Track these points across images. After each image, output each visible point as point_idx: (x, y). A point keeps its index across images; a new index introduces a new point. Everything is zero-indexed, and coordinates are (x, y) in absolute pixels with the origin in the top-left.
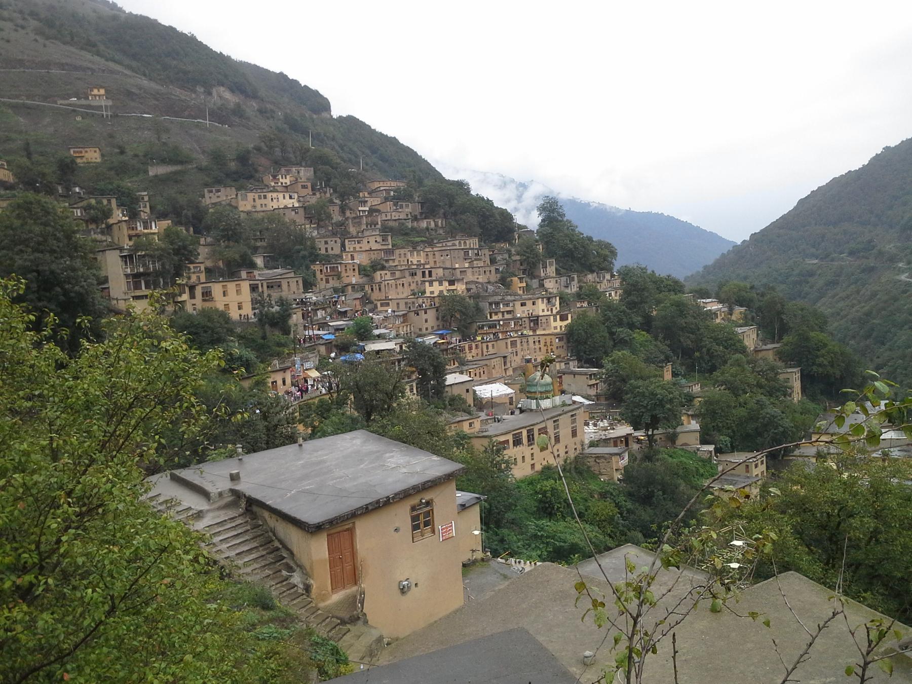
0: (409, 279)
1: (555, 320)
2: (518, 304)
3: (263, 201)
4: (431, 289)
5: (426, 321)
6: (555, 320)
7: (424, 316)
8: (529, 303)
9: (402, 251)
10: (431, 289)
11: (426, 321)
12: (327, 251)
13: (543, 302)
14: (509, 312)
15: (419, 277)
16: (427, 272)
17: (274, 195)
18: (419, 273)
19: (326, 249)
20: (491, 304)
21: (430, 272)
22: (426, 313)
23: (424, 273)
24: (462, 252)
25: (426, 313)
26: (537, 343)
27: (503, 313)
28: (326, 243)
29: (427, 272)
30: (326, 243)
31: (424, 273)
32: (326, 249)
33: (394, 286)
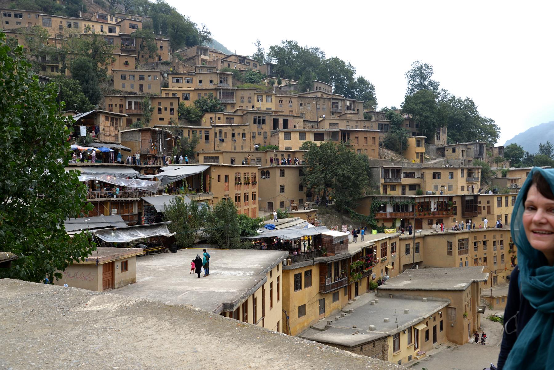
0: (255, 128)
1: (499, 205)
2: (428, 175)
4: (287, 143)
5: (282, 189)
6: (499, 205)
7: (280, 181)
8: (445, 175)
9: (246, 94)
10: (287, 143)
11: (282, 189)
13: (462, 176)
14: (412, 187)
15: (268, 127)
16: (281, 122)
18: (269, 122)
19: (141, 86)
20: (386, 171)
21: (285, 122)
22: (282, 174)
23: (276, 122)
24: (330, 104)
25: (282, 174)
26: (498, 246)
27: (404, 187)
28: (142, 78)
29: (281, 122)
30: (142, 78)
31: (276, 122)
32: (141, 86)
33: (229, 136)
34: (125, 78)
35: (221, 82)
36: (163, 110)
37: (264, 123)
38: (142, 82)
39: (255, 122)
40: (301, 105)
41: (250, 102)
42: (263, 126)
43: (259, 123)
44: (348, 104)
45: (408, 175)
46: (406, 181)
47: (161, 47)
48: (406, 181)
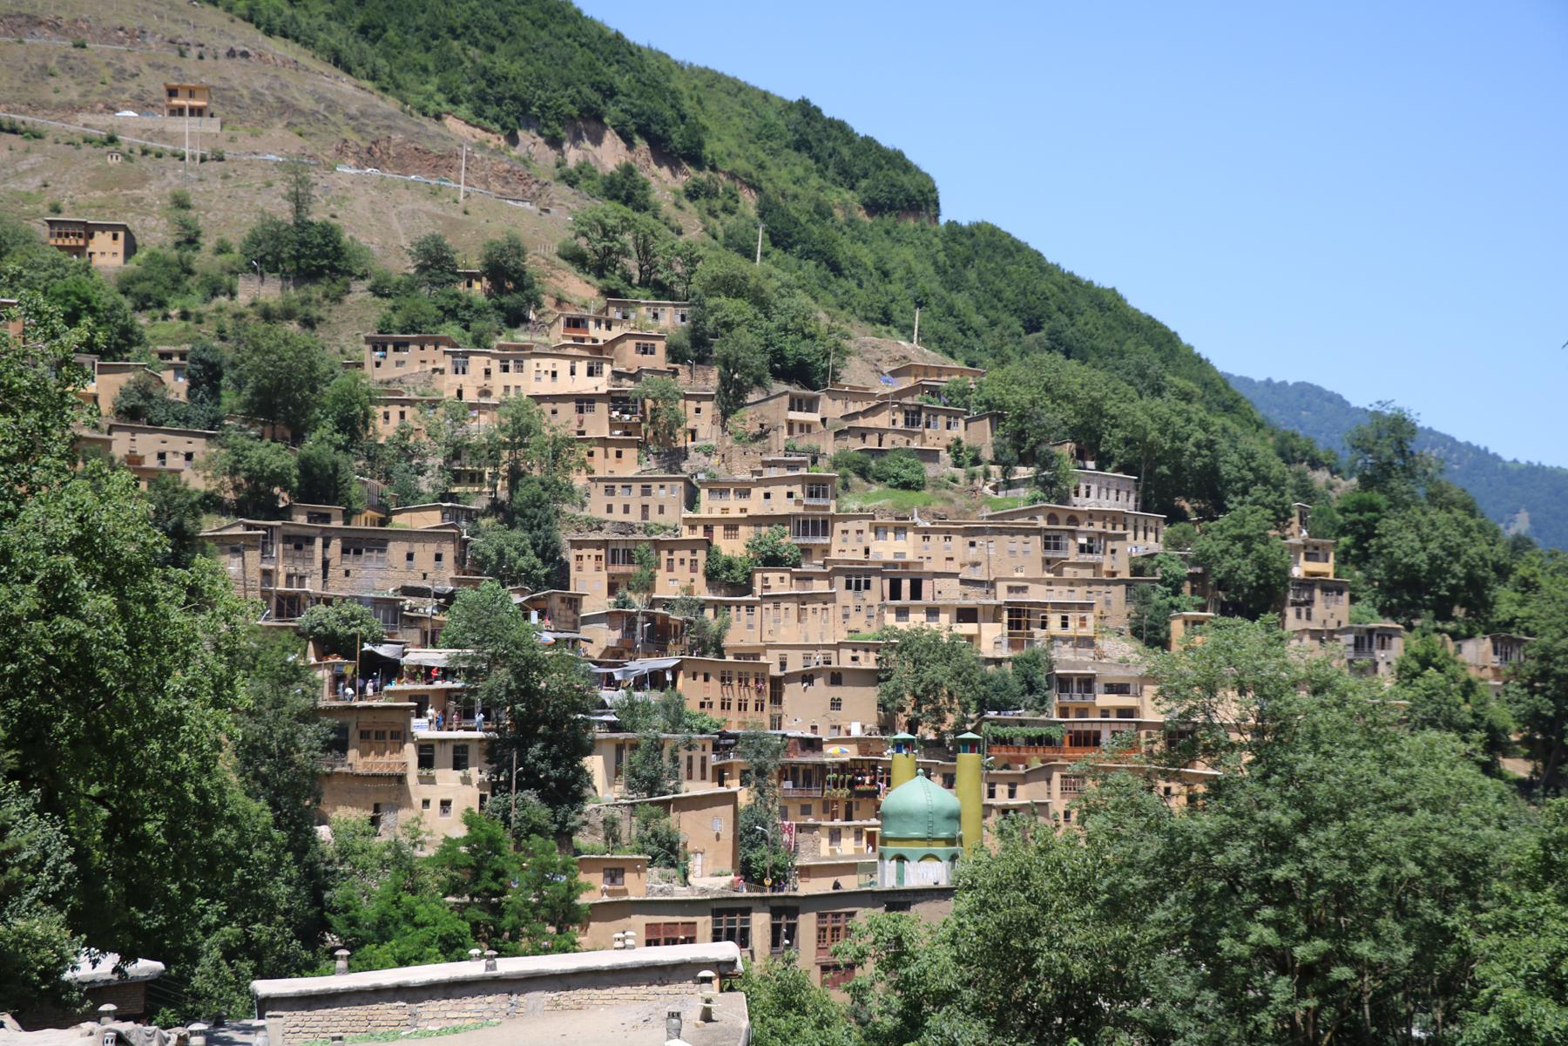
3: (512, 378)
12: (645, 515)
16: (906, 585)
17: (547, 364)
18: (880, 585)
19: (645, 508)
27: (1105, 712)
29: (906, 585)
32: (645, 508)
34: (613, 493)
35: (811, 495)
36: (677, 563)
37: (867, 587)
38: (646, 500)
39: (848, 587)
40: (972, 544)
41: (860, 540)
42: (865, 593)
43: (858, 588)
44: (1083, 541)
45: (1112, 689)
46: (1104, 700)
47: (698, 411)
48: (1104, 700)
